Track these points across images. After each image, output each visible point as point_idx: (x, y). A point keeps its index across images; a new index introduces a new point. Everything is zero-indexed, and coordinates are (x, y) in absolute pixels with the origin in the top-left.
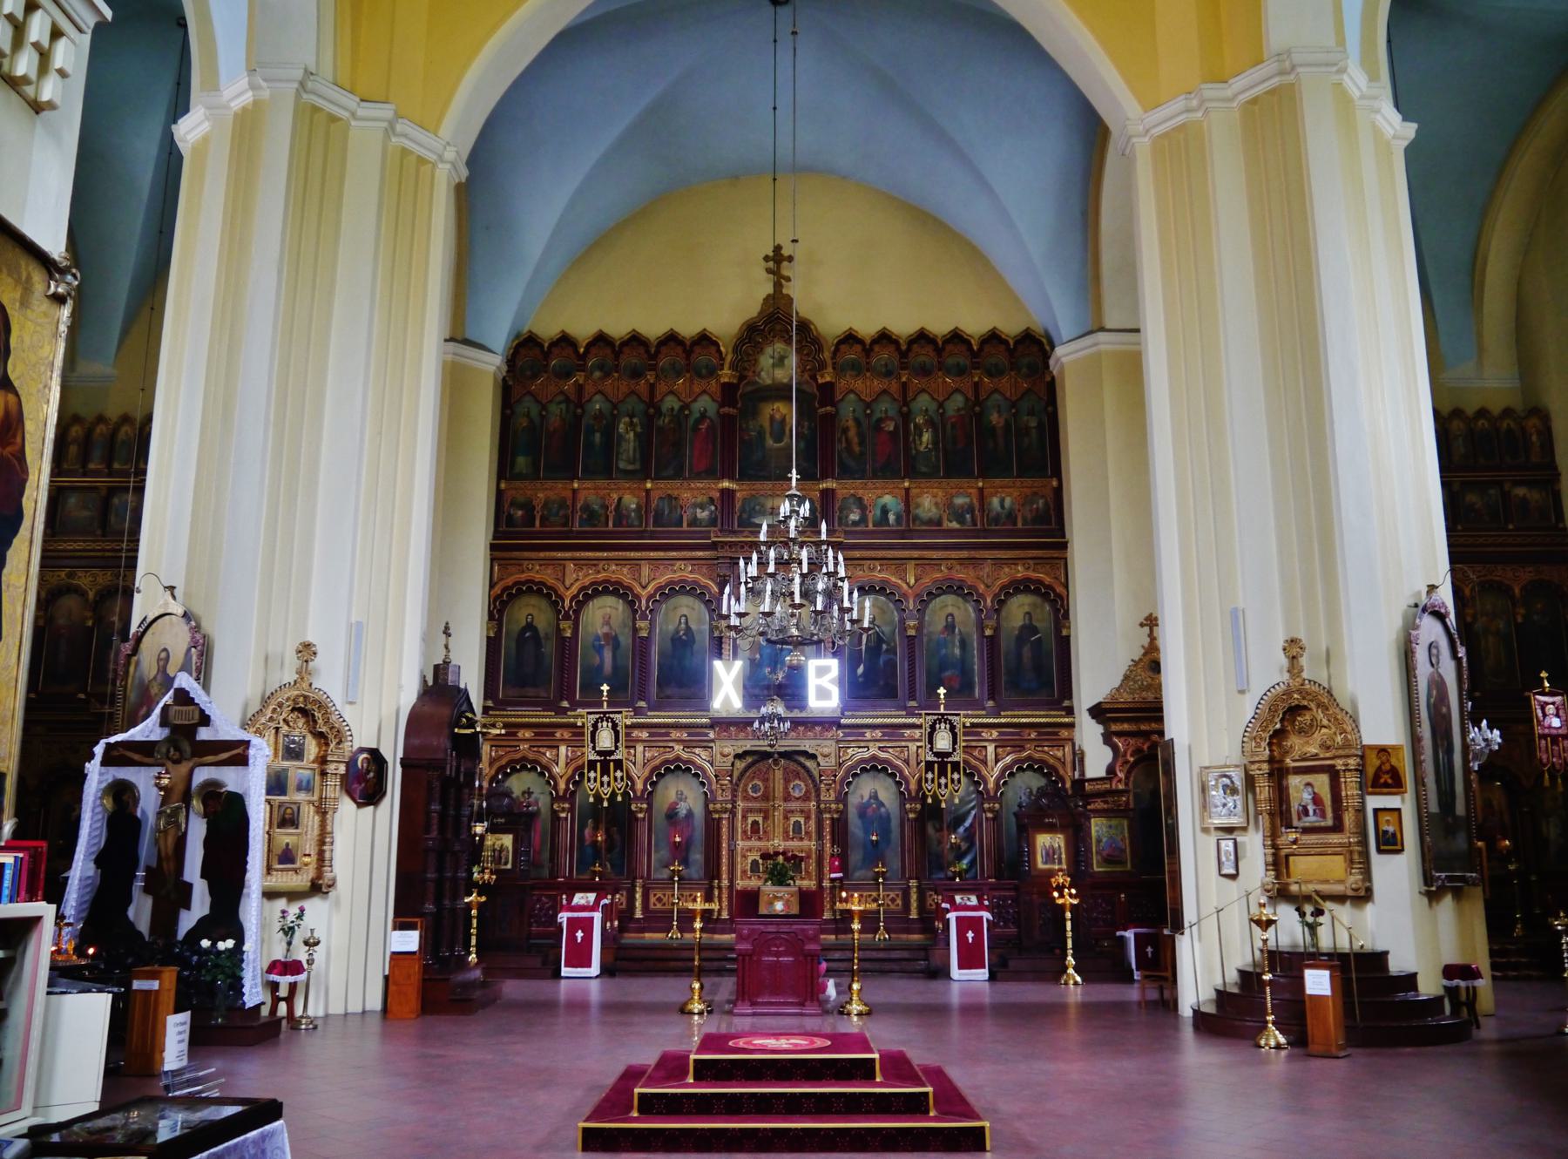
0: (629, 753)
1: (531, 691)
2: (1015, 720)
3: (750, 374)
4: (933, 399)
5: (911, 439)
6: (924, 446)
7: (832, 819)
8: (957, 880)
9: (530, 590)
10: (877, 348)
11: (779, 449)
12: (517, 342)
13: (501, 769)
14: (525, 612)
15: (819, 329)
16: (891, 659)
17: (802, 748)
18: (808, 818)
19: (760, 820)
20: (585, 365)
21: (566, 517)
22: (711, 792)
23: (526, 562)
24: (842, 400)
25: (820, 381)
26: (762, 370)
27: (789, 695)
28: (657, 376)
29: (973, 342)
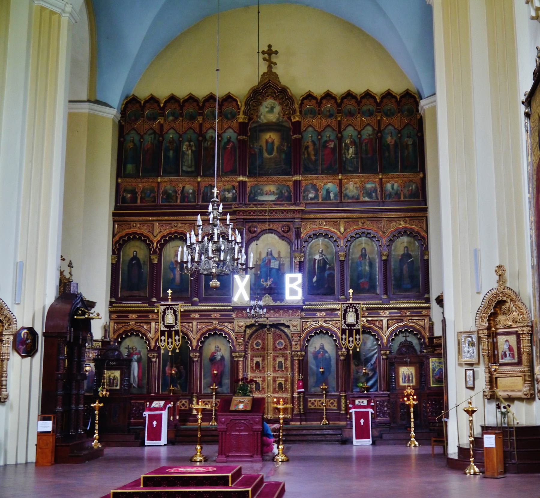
0: (189, 326)
1: (136, 293)
2: (398, 306)
3: (255, 117)
4: (355, 129)
5: (343, 151)
6: (350, 156)
7: (299, 360)
8: (366, 392)
9: (135, 238)
10: (324, 102)
11: (270, 159)
12: (126, 101)
13: (120, 335)
14: (132, 250)
15: (293, 92)
16: (331, 273)
17: (282, 322)
18: (286, 360)
19: (260, 361)
20: (164, 113)
21: (154, 197)
22: (233, 346)
23: (133, 223)
24: (305, 131)
25: (293, 120)
26: (261, 115)
27: (275, 293)
28: (203, 119)
29: (377, 97)
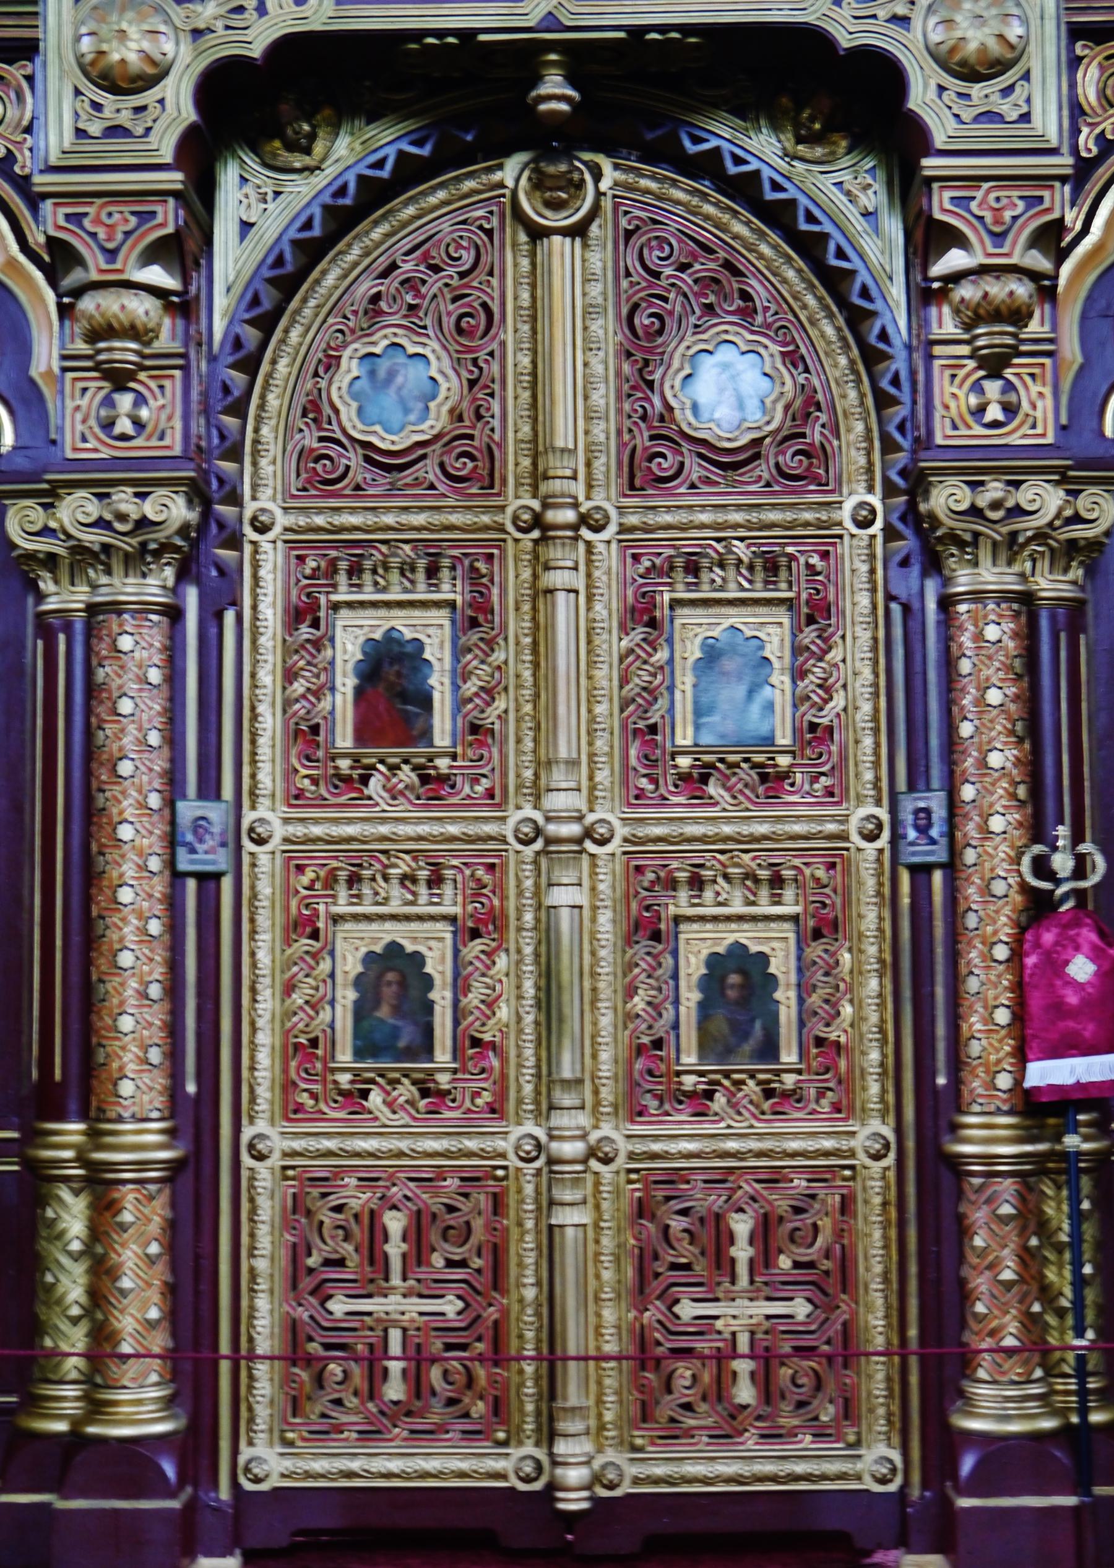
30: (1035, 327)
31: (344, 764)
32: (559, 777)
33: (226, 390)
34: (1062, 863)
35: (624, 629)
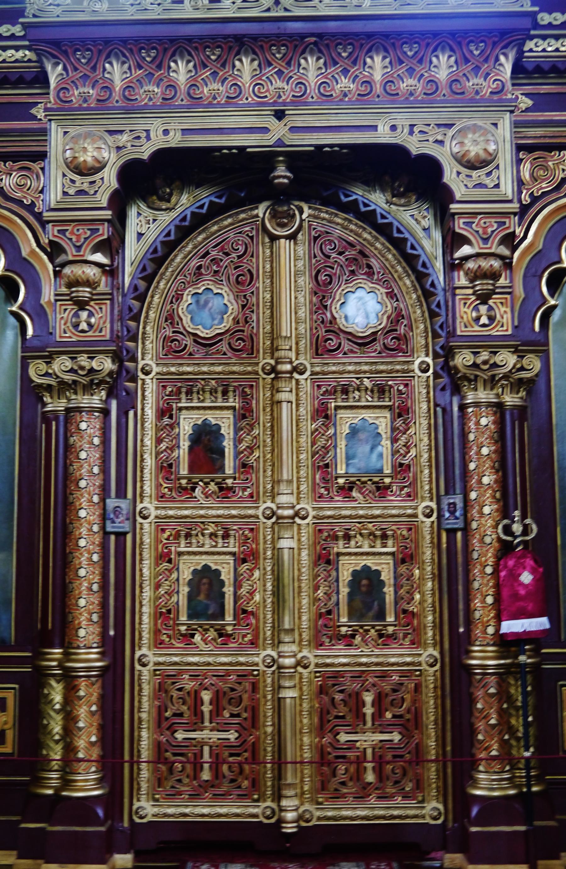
7: (499, 407)
30: (502, 281)
31: (184, 482)
32: (283, 488)
33: (130, 310)
34: (517, 528)
35: (313, 419)
